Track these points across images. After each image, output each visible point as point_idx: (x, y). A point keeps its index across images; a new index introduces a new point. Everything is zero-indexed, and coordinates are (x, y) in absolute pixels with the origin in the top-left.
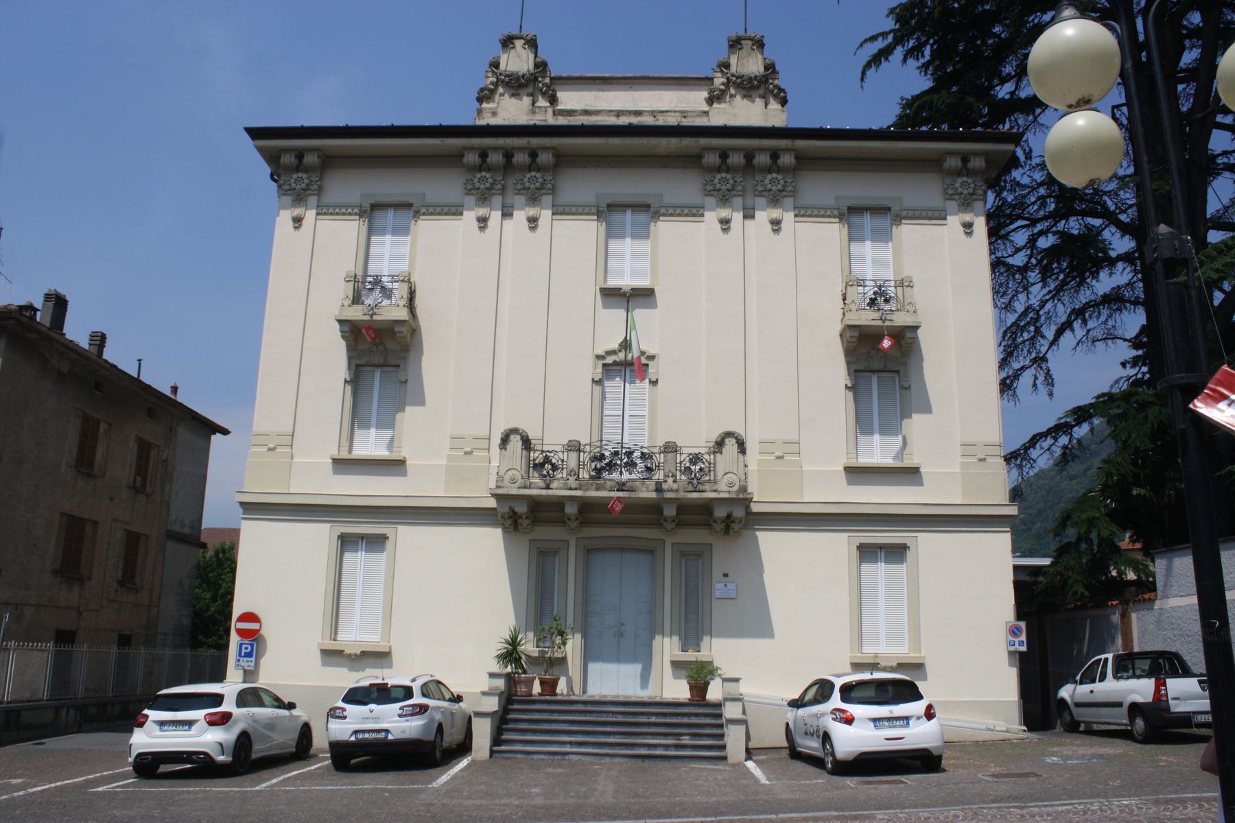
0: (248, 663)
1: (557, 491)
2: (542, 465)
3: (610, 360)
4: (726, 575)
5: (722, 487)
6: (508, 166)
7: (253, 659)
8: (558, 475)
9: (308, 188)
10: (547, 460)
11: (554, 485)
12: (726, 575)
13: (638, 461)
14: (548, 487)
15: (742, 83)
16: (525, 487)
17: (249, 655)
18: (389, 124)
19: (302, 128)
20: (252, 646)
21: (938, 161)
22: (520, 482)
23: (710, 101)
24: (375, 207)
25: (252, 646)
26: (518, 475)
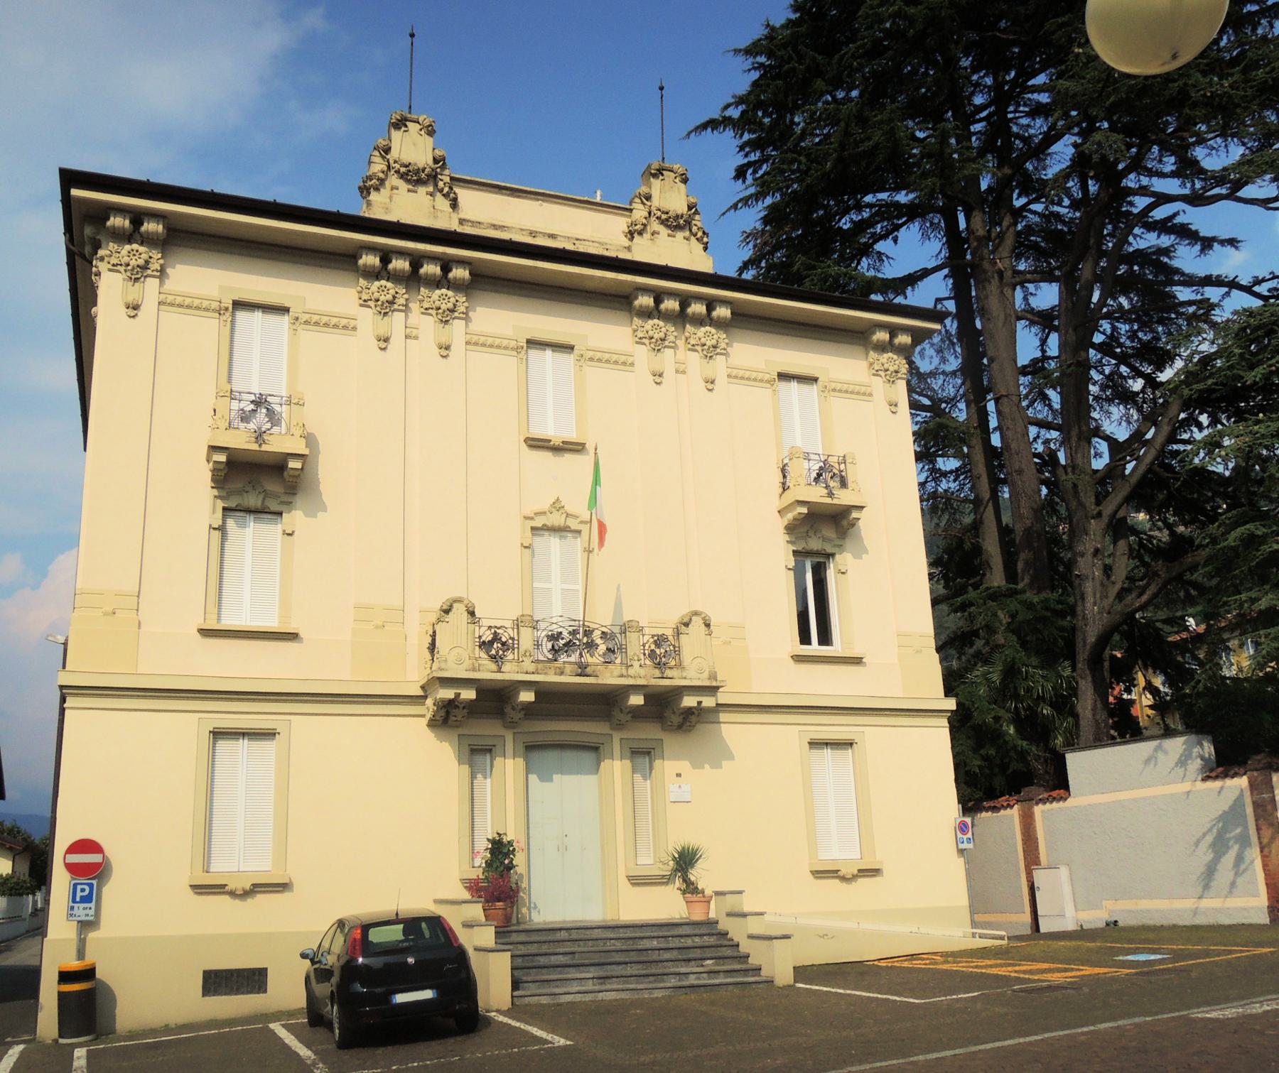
0: (82, 912)
1: (510, 672)
2: (491, 643)
3: (538, 523)
4: (679, 775)
5: (690, 672)
6: (412, 279)
7: (93, 905)
8: (510, 656)
9: (145, 267)
10: (496, 638)
11: (506, 668)
12: (679, 775)
13: (599, 641)
14: (499, 671)
15: (667, 220)
16: (474, 670)
17: (86, 899)
18: (335, 210)
19: (666, 267)
20: (91, 886)
21: (862, 333)
22: (467, 663)
23: (631, 235)
24: (238, 305)
25: (91, 886)
26: (465, 655)
